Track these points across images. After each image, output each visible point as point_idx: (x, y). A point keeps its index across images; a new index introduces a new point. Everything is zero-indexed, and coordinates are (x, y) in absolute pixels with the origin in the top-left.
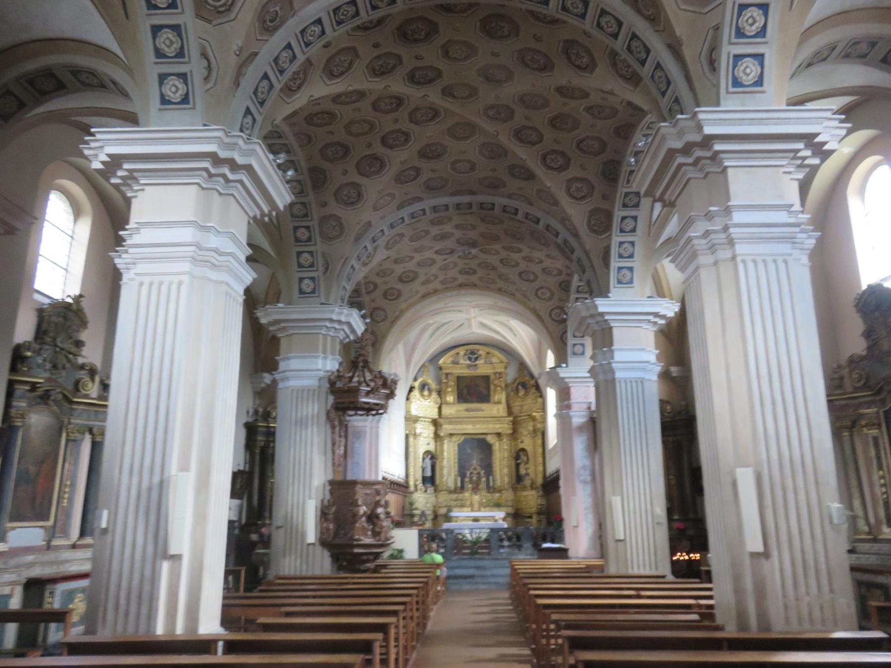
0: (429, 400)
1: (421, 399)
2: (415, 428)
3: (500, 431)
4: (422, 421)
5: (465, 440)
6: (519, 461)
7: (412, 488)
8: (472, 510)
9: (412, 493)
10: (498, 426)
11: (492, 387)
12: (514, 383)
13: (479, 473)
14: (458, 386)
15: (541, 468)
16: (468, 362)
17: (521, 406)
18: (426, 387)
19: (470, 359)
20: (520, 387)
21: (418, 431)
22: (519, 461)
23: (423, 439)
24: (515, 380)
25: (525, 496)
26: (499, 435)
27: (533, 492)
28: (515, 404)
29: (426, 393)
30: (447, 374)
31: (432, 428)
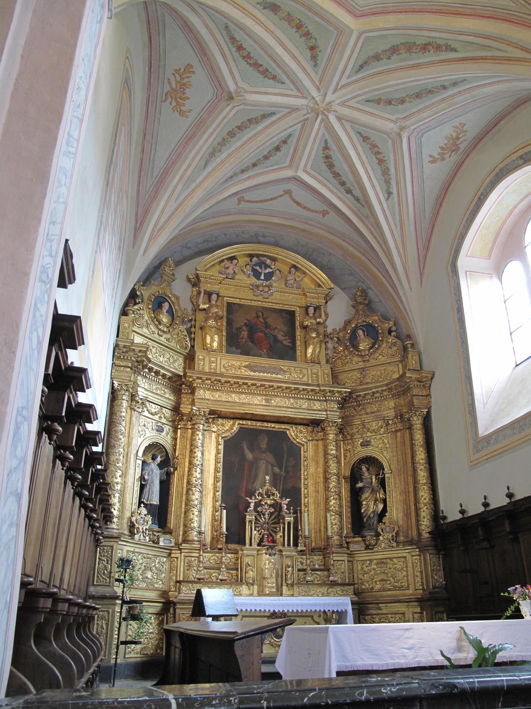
0: (168, 336)
1: (152, 327)
2: (136, 385)
3: (322, 415)
4: (150, 370)
5: (242, 430)
6: (360, 485)
7: (115, 526)
8: (261, 593)
9: (118, 538)
10: (317, 405)
11: (299, 332)
12: (344, 328)
13: (277, 506)
14: (229, 323)
15: (424, 495)
16: (254, 280)
17: (363, 370)
18: (166, 306)
19: (257, 275)
20: (360, 332)
21: (141, 393)
22: (360, 485)
23: (146, 413)
24: (348, 323)
25: (381, 562)
26: (315, 423)
27: (406, 552)
28: (347, 368)
29: (165, 319)
30: (209, 294)
31: (170, 396)
